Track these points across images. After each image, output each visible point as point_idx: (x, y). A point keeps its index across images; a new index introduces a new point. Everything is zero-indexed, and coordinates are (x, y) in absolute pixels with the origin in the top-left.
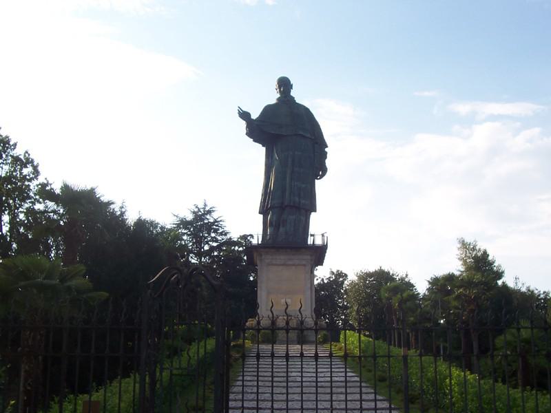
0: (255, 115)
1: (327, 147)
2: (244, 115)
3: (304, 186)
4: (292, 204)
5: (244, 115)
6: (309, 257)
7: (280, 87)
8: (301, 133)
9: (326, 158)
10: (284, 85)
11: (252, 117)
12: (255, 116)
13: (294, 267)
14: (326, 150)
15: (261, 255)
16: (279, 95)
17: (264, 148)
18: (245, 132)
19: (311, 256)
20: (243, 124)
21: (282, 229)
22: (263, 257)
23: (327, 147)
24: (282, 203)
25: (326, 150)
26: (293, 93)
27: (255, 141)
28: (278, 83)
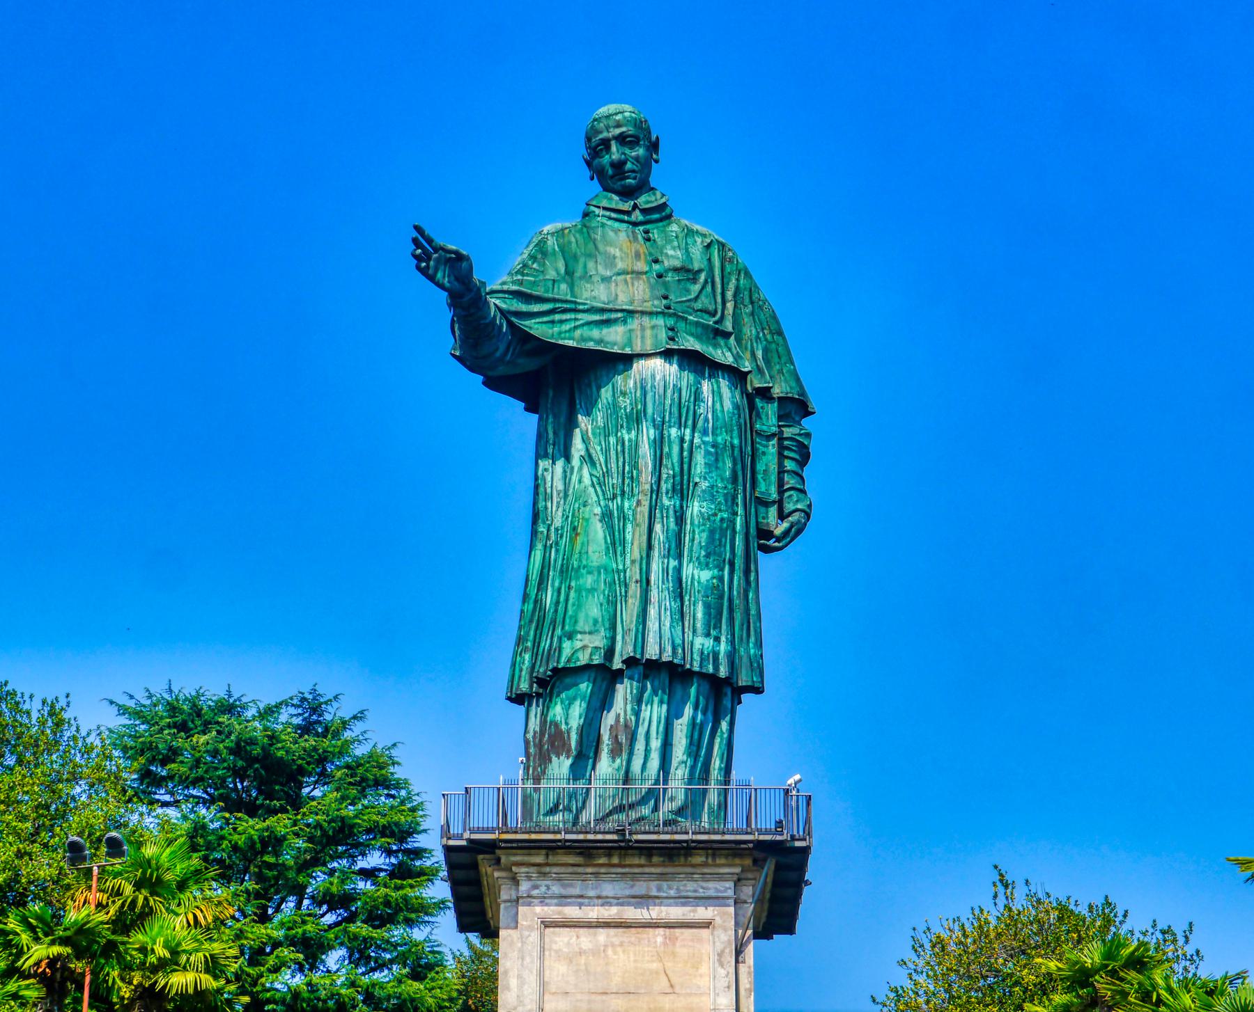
3: (706, 575)
4: (652, 652)
6: (727, 888)
13: (659, 935)
15: (515, 881)
19: (738, 881)
21: (606, 766)
22: (524, 886)
24: (610, 653)
27: (493, 383)
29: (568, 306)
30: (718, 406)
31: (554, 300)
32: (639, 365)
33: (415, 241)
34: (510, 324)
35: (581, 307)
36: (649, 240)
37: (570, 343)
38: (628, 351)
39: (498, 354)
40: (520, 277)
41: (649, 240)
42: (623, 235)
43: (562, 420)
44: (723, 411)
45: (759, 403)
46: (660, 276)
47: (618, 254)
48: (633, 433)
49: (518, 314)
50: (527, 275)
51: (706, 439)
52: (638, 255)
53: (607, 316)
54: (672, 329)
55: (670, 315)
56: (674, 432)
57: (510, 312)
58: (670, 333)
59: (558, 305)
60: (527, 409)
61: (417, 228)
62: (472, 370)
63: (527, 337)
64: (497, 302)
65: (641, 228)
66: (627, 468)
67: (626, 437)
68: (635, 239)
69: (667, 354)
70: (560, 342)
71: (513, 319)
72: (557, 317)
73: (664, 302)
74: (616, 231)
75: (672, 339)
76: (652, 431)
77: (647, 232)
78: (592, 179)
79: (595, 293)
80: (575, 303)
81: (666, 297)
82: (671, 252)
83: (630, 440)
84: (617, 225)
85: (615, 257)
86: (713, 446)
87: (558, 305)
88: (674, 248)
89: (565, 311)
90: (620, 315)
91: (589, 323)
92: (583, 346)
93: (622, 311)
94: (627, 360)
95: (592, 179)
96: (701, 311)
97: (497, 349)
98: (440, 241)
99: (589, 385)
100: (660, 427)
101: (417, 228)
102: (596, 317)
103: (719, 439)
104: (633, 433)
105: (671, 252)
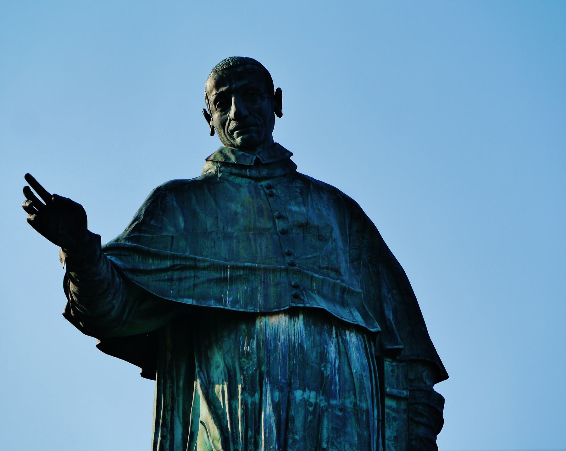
0: (109, 223)
1: (442, 375)
2: (56, 217)
5: (56, 217)
7: (222, 102)
8: (322, 304)
9: (438, 424)
10: (247, 93)
11: (92, 227)
12: (109, 223)
14: (438, 388)
16: (216, 144)
17: (152, 385)
18: (64, 301)
20: (50, 259)
23: (442, 375)
25: (438, 388)
26: (282, 133)
28: (218, 84)
29: (188, 263)
30: (346, 368)
31: (174, 257)
32: (260, 322)
33: (26, 191)
34: (128, 282)
35: (201, 265)
36: (272, 195)
37: (190, 302)
38: (250, 309)
39: (113, 313)
40: (137, 234)
41: (272, 195)
42: (244, 191)
43: (181, 384)
44: (351, 373)
45: (388, 365)
46: (284, 232)
47: (239, 210)
48: (257, 396)
49: (135, 271)
50: (145, 232)
51: (334, 402)
52: (260, 212)
53: (227, 275)
54: (296, 287)
55: (295, 272)
56: (298, 394)
57: (126, 269)
58: (295, 291)
59: (177, 262)
60: (143, 375)
61: (29, 177)
62: (86, 331)
63: (144, 295)
64: (113, 259)
65: (264, 183)
66: (250, 433)
67: (249, 401)
68: (258, 194)
69: (292, 313)
70: (180, 301)
71: (130, 276)
72: (176, 275)
73: (288, 259)
74: (238, 187)
75: (296, 296)
76: (277, 394)
77: (269, 187)
78: (212, 134)
79: (216, 252)
80: (195, 259)
81: (289, 254)
82: (295, 208)
83: (253, 403)
84: (238, 180)
85: (236, 213)
86: (341, 410)
87: (177, 262)
88: (298, 204)
89: (183, 268)
90: (241, 273)
91: (209, 281)
92: (204, 304)
93: (244, 268)
94: (250, 318)
95: (212, 134)
96: (327, 268)
97: (113, 307)
98: (51, 191)
99: (209, 347)
100: (287, 389)
101: (29, 177)
102: (216, 275)
103: (348, 403)
104: (257, 396)
105: (295, 208)
